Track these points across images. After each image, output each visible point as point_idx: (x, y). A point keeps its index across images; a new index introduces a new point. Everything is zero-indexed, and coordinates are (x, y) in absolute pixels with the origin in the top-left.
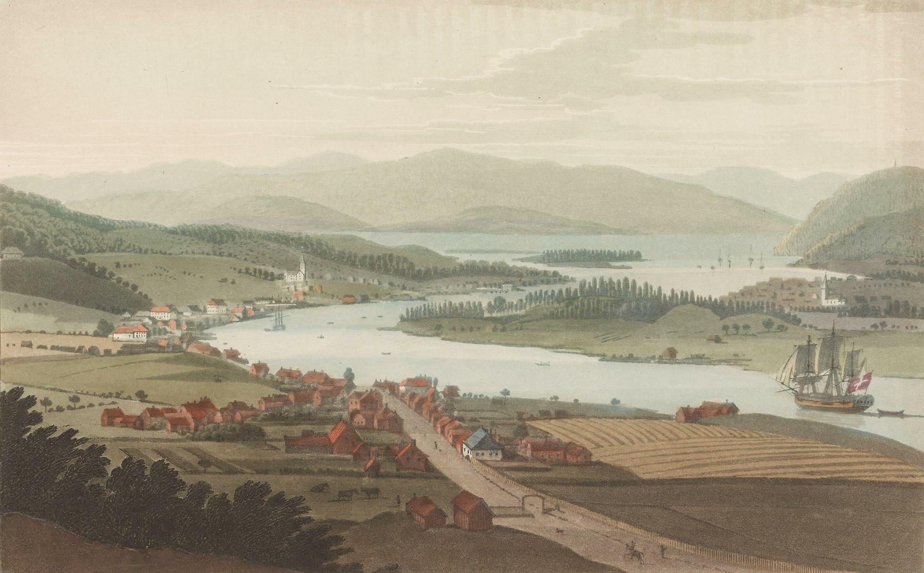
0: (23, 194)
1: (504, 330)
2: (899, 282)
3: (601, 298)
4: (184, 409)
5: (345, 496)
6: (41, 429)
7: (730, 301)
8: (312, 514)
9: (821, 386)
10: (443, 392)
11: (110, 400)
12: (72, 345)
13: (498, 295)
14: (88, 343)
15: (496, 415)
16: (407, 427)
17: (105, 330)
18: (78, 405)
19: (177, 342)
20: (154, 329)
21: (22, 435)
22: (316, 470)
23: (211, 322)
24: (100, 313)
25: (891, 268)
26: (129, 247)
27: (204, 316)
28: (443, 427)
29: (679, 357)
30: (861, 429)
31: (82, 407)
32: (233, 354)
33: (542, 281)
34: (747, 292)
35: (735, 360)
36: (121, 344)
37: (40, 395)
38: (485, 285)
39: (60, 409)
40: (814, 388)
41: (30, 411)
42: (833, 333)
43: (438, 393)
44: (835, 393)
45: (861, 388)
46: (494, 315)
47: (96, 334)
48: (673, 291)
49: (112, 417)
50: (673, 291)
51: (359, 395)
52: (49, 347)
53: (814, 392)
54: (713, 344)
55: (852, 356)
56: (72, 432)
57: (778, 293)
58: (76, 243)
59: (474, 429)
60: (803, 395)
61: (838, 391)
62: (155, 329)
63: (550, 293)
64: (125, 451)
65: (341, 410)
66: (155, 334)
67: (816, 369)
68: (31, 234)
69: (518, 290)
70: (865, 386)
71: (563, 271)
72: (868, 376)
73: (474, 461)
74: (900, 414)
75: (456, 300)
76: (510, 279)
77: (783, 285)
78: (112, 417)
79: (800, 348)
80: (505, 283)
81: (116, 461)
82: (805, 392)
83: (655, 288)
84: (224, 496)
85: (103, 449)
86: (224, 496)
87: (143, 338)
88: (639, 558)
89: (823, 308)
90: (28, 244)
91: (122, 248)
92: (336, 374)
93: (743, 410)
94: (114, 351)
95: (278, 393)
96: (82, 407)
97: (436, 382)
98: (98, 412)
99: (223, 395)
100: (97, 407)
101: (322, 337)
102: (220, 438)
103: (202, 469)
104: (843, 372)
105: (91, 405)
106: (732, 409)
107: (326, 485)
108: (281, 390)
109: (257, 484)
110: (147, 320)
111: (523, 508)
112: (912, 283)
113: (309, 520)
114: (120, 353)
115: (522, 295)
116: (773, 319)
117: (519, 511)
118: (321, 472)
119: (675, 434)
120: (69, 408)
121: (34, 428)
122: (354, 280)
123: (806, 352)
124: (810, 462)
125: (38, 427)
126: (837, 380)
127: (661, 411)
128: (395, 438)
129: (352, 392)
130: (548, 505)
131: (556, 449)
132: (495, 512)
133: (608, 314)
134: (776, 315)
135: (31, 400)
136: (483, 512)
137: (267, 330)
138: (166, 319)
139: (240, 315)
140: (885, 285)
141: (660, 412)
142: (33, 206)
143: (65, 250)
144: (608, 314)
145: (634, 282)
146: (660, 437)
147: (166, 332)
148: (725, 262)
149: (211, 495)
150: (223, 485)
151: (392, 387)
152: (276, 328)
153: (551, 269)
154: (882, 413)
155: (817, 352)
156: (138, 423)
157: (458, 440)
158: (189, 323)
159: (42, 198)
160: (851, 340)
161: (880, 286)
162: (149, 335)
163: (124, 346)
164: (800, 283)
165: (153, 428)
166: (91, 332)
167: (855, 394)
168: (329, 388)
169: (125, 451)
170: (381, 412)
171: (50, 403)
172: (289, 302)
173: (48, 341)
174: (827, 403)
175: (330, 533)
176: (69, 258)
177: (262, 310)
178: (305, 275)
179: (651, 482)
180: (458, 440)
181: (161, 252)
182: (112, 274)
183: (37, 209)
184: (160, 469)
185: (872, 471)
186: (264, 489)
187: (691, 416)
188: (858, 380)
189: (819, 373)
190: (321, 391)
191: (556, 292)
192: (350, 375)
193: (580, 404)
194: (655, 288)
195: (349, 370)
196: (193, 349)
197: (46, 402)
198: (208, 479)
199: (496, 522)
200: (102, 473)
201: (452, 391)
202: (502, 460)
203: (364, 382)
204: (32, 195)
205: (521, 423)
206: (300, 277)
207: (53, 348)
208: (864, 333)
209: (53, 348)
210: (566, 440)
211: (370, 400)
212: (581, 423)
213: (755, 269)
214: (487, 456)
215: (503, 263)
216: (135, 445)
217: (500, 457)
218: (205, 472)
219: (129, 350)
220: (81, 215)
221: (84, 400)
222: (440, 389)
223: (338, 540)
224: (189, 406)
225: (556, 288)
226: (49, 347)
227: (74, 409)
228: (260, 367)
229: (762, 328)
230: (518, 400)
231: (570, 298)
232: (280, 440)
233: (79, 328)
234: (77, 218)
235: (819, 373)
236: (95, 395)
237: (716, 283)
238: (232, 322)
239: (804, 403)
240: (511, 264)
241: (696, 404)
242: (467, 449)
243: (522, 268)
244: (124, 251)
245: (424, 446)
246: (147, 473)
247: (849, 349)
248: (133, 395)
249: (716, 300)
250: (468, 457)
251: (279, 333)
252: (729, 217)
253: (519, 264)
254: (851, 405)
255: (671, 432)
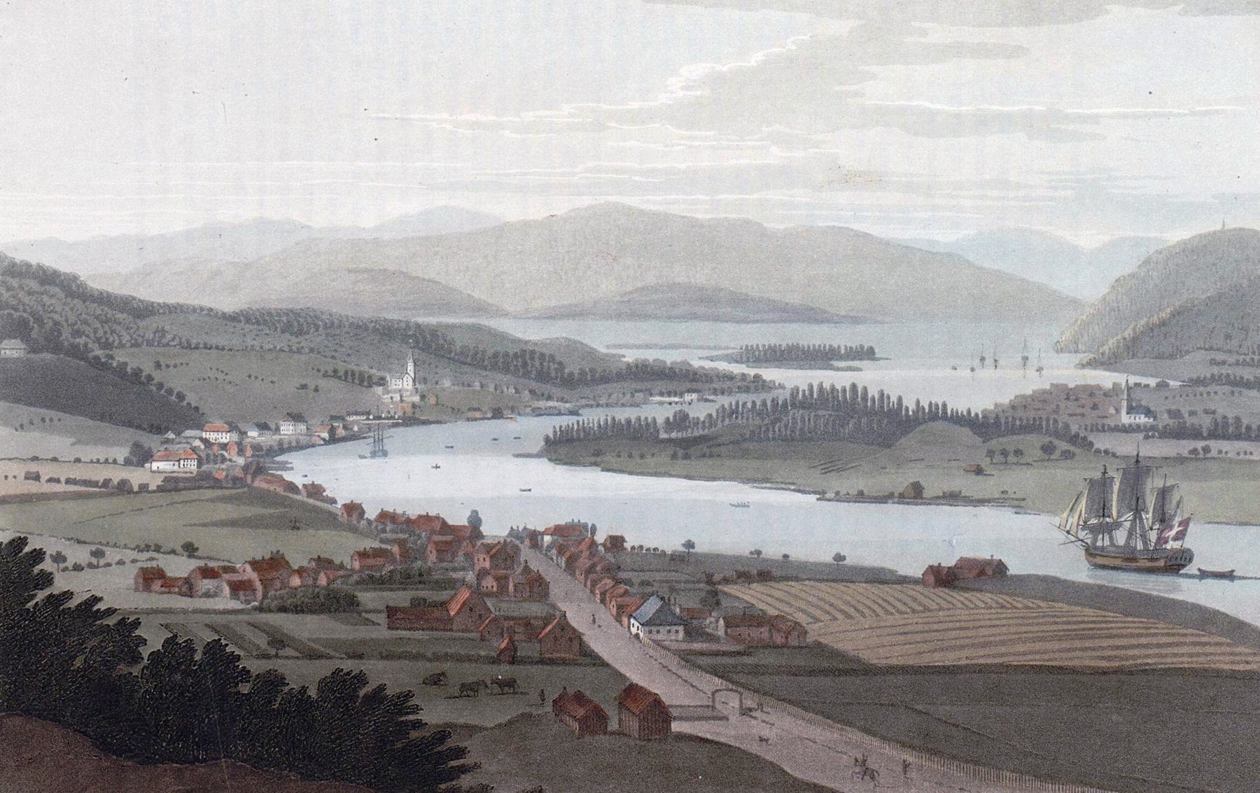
0: (29, 266)
1: (687, 457)
2: (1227, 388)
3: (820, 413)
4: (248, 568)
5: (469, 690)
6: (51, 596)
7: (997, 417)
8: (424, 716)
9: (1121, 537)
10: (604, 545)
11: (147, 555)
12: (94, 478)
13: (678, 408)
14: (117, 475)
15: (673, 576)
16: (556, 592)
17: (142, 457)
18: (102, 562)
19: (238, 473)
20: (208, 455)
21: (24, 604)
22: (429, 654)
23: (285, 446)
24: (130, 434)
25: (1216, 370)
26: (173, 340)
27: (277, 437)
28: (603, 594)
29: (926, 494)
30: (1179, 597)
31: (109, 565)
32: (315, 491)
33: (739, 388)
34: (1021, 404)
35: (1002, 500)
36: (162, 477)
37: (51, 546)
38: (661, 394)
39: (78, 568)
40: (1111, 538)
41: (36, 569)
42: (1137, 461)
43: (597, 546)
44: (1140, 546)
45: (1176, 539)
46: (674, 435)
47: (128, 462)
48: (918, 402)
49: (151, 578)
50: (918, 402)
51: (488, 548)
52: (63, 480)
53: (1112, 544)
54: (973, 477)
55: (1164, 494)
56: (96, 600)
57: (1062, 406)
58: (100, 333)
59: (645, 598)
60: (1096, 548)
61: (1145, 543)
62: (210, 453)
63: (749, 405)
64: (167, 626)
65: (464, 569)
66: (208, 462)
67: (1114, 513)
68: (39, 320)
69: (707, 400)
70: (1180, 536)
71: (770, 374)
72: (1185, 523)
73: (646, 640)
74: (1229, 576)
75: (622, 414)
76: (695, 385)
77: (1069, 394)
78: (151, 578)
79: (1092, 482)
80: (688, 391)
81: (154, 640)
82: (1099, 543)
83: (894, 399)
84: (304, 689)
85: (137, 623)
86: (304, 689)
87: (192, 466)
88: (873, 778)
89: (1124, 425)
90: (34, 335)
91: (164, 341)
92: (458, 518)
93: (1014, 569)
94: (153, 487)
95: (376, 545)
96: (109, 565)
97: (594, 529)
98: (131, 572)
99: (299, 550)
100: (128, 565)
101: (437, 467)
102: (298, 609)
103: (273, 652)
104: (1150, 515)
105: (121, 563)
106: (999, 568)
107: (443, 674)
108: (382, 541)
109: (348, 674)
110: (197, 443)
111: (713, 707)
112: (1245, 391)
113: (418, 724)
114: (160, 489)
115: (711, 409)
116: (1056, 442)
117: (708, 713)
118: (437, 658)
119: (920, 604)
120: (91, 566)
121: (41, 595)
122: (482, 386)
123: (1100, 488)
124: (1105, 643)
125: (47, 592)
126: (1142, 527)
127: (903, 571)
128: (535, 609)
129: (479, 543)
130: (749, 703)
131: (760, 625)
132: (674, 712)
133: (852, 437)
134: (1057, 434)
135: (38, 555)
136: (656, 713)
137: (362, 457)
138: (225, 441)
139: (326, 435)
140: (1208, 393)
141: (901, 573)
142: (42, 283)
143: (86, 345)
144: (852, 437)
145: (865, 389)
146: (903, 608)
147: (224, 460)
148: (989, 361)
149: (286, 689)
150: (304, 675)
151: (534, 537)
152: (374, 455)
153: (752, 372)
154: (1203, 575)
155: (1116, 487)
156: (187, 587)
157: (623, 612)
158: (256, 448)
159: (55, 272)
160: (1161, 471)
161: (1201, 395)
162: (200, 465)
163: (166, 480)
164: (1091, 391)
165: (207, 595)
166: (121, 460)
167: (1169, 547)
168: (449, 538)
169: (167, 626)
170: (519, 570)
171: (65, 559)
172: (392, 418)
173: (64, 473)
174: (1128, 560)
175: (451, 743)
176: (91, 355)
177: (356, 428)
178: (414, 381)
179: (892, 670)
180: (623, 612)
181: (217, 348)
182: (150, 378)
183: (47, 287)
184: (214, 648)
185: (1191, 655)
186: (361, 679)
187: (944, 578)
188: (1171, 528)
189: (1119, 517)
190: (435, 543)
191: (758, 403)
192: (475, 521)
193: (791, 562)
194: (894, 399)
195: (475, 513)
196: (259, 483)
197: (59, 558)
198: (279, 666)
199: (676, 727)
200: (137, 658)
201: (616, 542)
202: (684, 641)
203: (494, 530)
204: (40, 267)
205: (709, 588)
206: (407, 383)
207: (68, 481)
208: (1180, 460)
209: (68, 481)
210: (772, 612)
211: (504, 553)
212: (795, 587)
213: (1031, 372)
214: (662, 635)
215: (686, 363)
216: (180, 619)
217: (681, 635)
218: (276, 656)
219: (172, 485)
220: (109, 295)
221: (112, 555)
222: (600, 538)
223: (460, 752)
224: (255, 565)
225: (758, 398)
226: (63, 480)
227: (97, 567)
228: (354, 509)
229: (1039, 453)
230: (706, 556)
231: (779, 409)
232: (380, 612)
233: (99, 455)
234: (104, 299)
235: (1119, 517)
236: (125, 547)
237: (979, 392)
238: (313, 446)
239: (1099, 560)
240: (696, 364)
241: (949, 561)
242: (637, 624)
243: (712, 369)
244: (167, 345)
245: (577, 618)
246: (198, 657)
247: (1159, 483)
248: (179, 550)
249: (977, 415)
250: (637, 635)
251: (378, 461)
252: (990, 299)
253: (708, 365)
254: (1161, 563)
255: (915, 600)
